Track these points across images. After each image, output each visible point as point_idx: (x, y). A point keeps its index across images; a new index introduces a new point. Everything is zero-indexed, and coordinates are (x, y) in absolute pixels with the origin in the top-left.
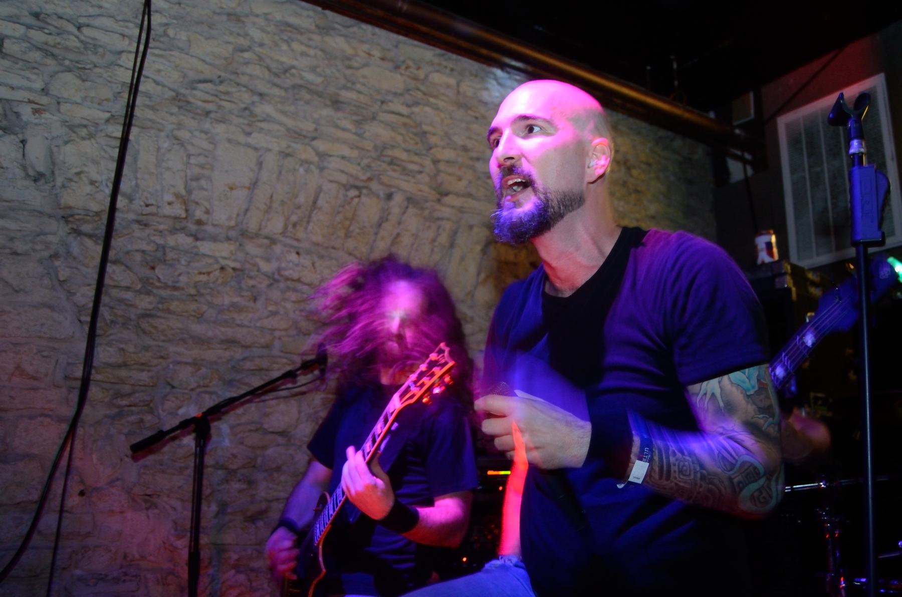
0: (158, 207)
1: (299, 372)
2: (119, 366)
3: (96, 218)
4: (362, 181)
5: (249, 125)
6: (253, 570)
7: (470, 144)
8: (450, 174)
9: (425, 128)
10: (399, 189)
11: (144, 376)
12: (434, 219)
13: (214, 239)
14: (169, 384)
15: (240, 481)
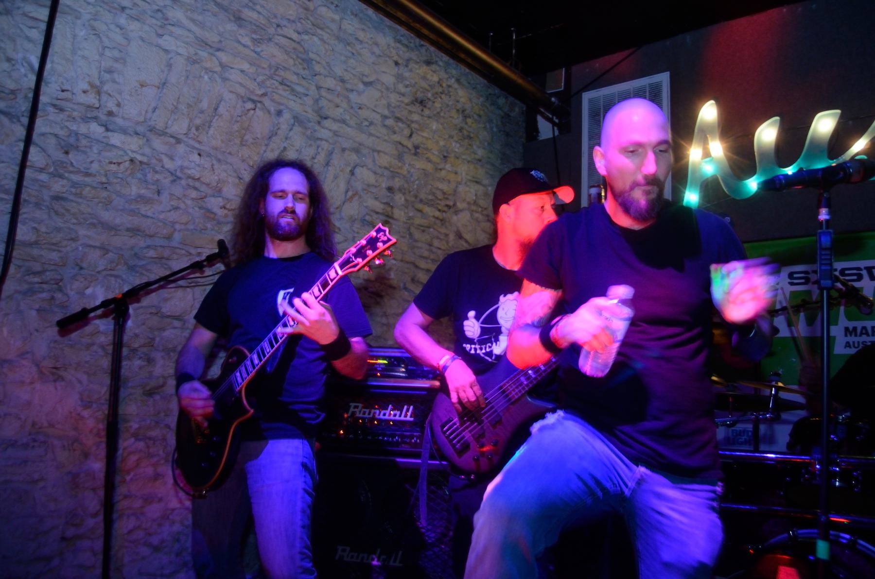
0: (73, 94)
1: (205, 263)
2: (31, 245)
3: (12, 96)
4: (257, 95)
5: (161, 27)
6: (150, 438)
7: (347, 77)
8: (330, 101)
9: (311, 55)
10: (287, 108)
11: (55, 256)
12: (314, 139)
13: (124, 131)
14: (77, 265)
15: (140, 358)
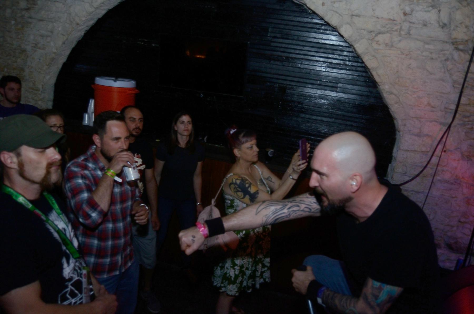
2: (466, 105)
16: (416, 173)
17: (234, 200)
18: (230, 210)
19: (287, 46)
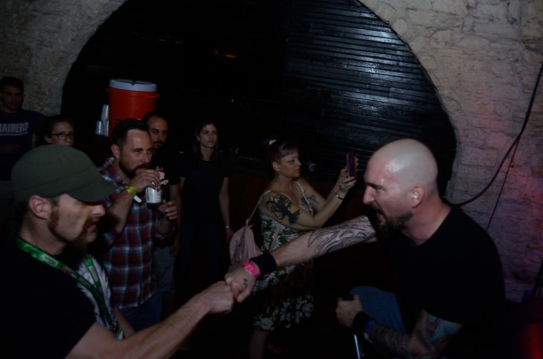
2: (538, 113)
16: (479, 191)
17: (271, 221)
18: (267, 233)
19: (331, 44)
